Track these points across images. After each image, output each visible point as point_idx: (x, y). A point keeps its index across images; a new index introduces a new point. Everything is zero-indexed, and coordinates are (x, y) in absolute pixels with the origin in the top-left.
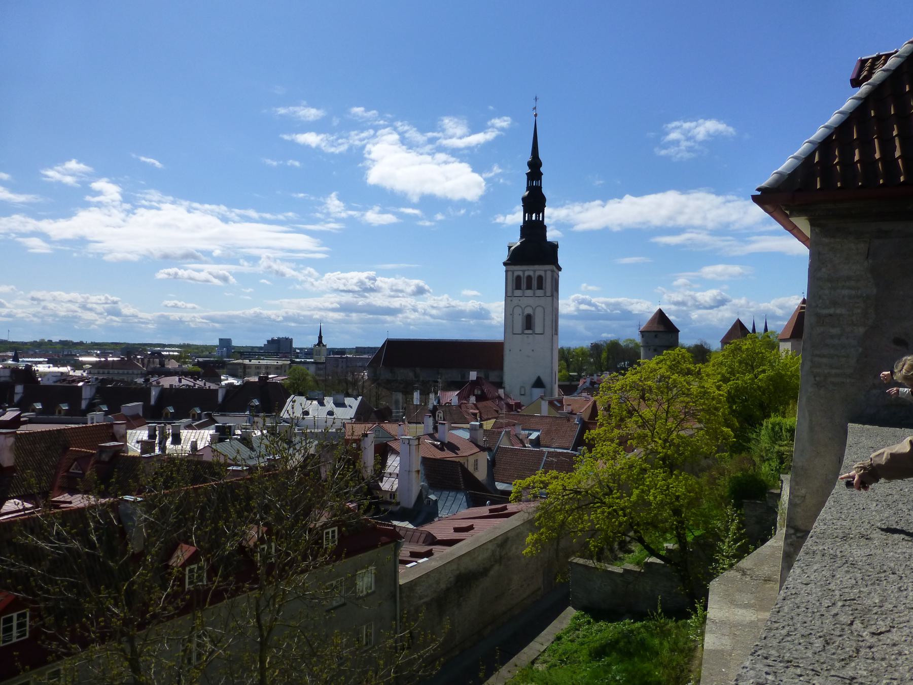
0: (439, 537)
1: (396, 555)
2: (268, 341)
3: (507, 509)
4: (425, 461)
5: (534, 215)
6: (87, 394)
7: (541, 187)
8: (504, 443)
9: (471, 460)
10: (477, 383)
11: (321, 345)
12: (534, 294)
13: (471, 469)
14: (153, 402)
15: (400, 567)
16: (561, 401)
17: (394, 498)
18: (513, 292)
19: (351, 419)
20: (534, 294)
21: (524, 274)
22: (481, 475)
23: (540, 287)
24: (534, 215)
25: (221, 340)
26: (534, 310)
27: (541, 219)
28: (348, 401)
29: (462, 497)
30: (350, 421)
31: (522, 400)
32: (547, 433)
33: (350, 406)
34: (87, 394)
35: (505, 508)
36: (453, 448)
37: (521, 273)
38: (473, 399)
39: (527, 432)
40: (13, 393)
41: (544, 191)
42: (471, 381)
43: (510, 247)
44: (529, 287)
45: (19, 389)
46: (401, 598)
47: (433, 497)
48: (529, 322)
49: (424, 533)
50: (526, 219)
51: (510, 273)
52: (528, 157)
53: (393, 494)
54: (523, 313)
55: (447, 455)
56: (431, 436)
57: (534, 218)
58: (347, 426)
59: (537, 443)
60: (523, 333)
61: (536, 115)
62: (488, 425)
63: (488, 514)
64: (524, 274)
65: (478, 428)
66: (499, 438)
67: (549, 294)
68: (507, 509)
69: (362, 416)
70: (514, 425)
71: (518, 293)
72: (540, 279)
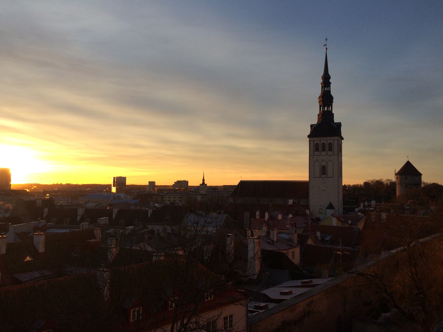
3: (312, 282)
4: (263, 251)
5: (326, 108)
6: (80, 212)
7: (330, 91)
12: (327, 153)
13: (290, 257)
14: (114, 217)
18: (314, 153)
20: (327, 153)
23: (330, 149)
24: (326, 108)
25: (149, 182)
27: (330, 110)
34: (80, 212)
35: (311, 282)
37: (318, 142)
41: (332, 93)
44: (324, 150)
45: (46, 210)
48: (324, 170)
51: (312, 142)
57: (326, 109)
60: (320, 177)
67: (336, 153)
68: (312, 282)
71: (317, 153)
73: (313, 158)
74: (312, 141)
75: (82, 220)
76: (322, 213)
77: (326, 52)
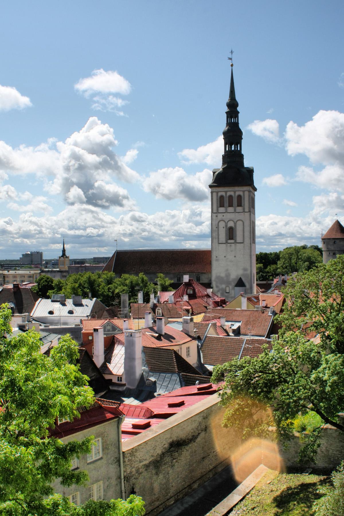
0: (156, 411)
1: (118, 427)
2: (23, 255)
5: (233, 146)
8: (211, 333)
9: (184, 347)
10: (188, 285)
11: (65, 256)
12: (235, 210)
15: (122, 437)
16: (257, 298)
17: (121, 380)
18: (218, 210)
19: (87, 316)
20: (235, 210)
21: (226, 194)
22: (192, 360)
23: (240, 204)
24: (233, 146)
26: (235, 224)
27: (239, 149)
28: (85, 301)
29: (175, 378)
30: (86, 318)
32: (247, 324)
33: (86, 305)
35: (210, 387)
36: (169, 338)
37: (224, 194)
38: (186, 298)
39: (230, 323)
41: (241, 126)
42: (185, 283)
43: (214, 173)
44: (231, 205)
46: (124, 462)
47: (153, 379)
48: (231, 233)
49: (143, 409)
50: (227, 150)
51: (215, 194)
52: (226, 98)
53: (120, 378)
54: (226, 226)
55: (164, 344)
56: (151, 329)
57: (233, 149)
58: (84, 322)
59: (237, 332)
60: (226, 243)
61: (232, 65)
62: (198, 318)
63: (196, 391)
64: (226, 194)
65: (189, 321)
66: (207, 329)
67: (247, 210)
68: (212, 388)
69: (95, 314)
70: (220, 318)
71: (222, 209)
72: (239, 197)
73: (217, 216)
74: (215, 192)
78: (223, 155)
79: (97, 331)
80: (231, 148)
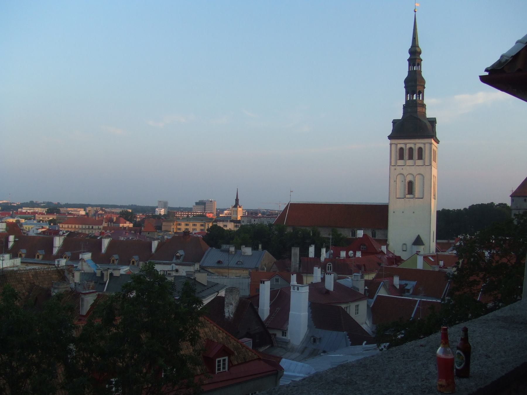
6: (58, 242)
14: (104, 250)
17: (285, 336)
18: (396, 163)
20: (415, 163)
21: (406, 146)
24: (415, 95)
26: (414, 177)
27: (421, 99)
31: (404, 256)
34: (58, 242)
37: (403, 146)
40: (7, 241)
41: (424, 75)
44: (411, 157)
45: (12, 238)
48: (410, 187)
50: (408, 99)
51: (393, 146)
52: (409, 45)
57: (415, 98)
60: (405, 197)
65: (359, 278)
71: (400, 162)
72: (420, 150)
74: (394, 144)
75: (61, 255)
76: (405, 251)
77: (415, 14)
78: (404, 105)
79: (264, 283)
80: (413, 97)
